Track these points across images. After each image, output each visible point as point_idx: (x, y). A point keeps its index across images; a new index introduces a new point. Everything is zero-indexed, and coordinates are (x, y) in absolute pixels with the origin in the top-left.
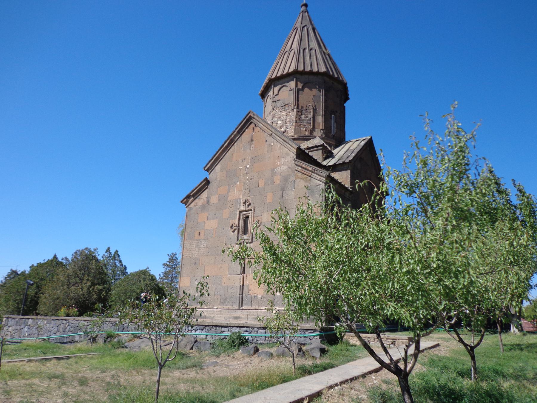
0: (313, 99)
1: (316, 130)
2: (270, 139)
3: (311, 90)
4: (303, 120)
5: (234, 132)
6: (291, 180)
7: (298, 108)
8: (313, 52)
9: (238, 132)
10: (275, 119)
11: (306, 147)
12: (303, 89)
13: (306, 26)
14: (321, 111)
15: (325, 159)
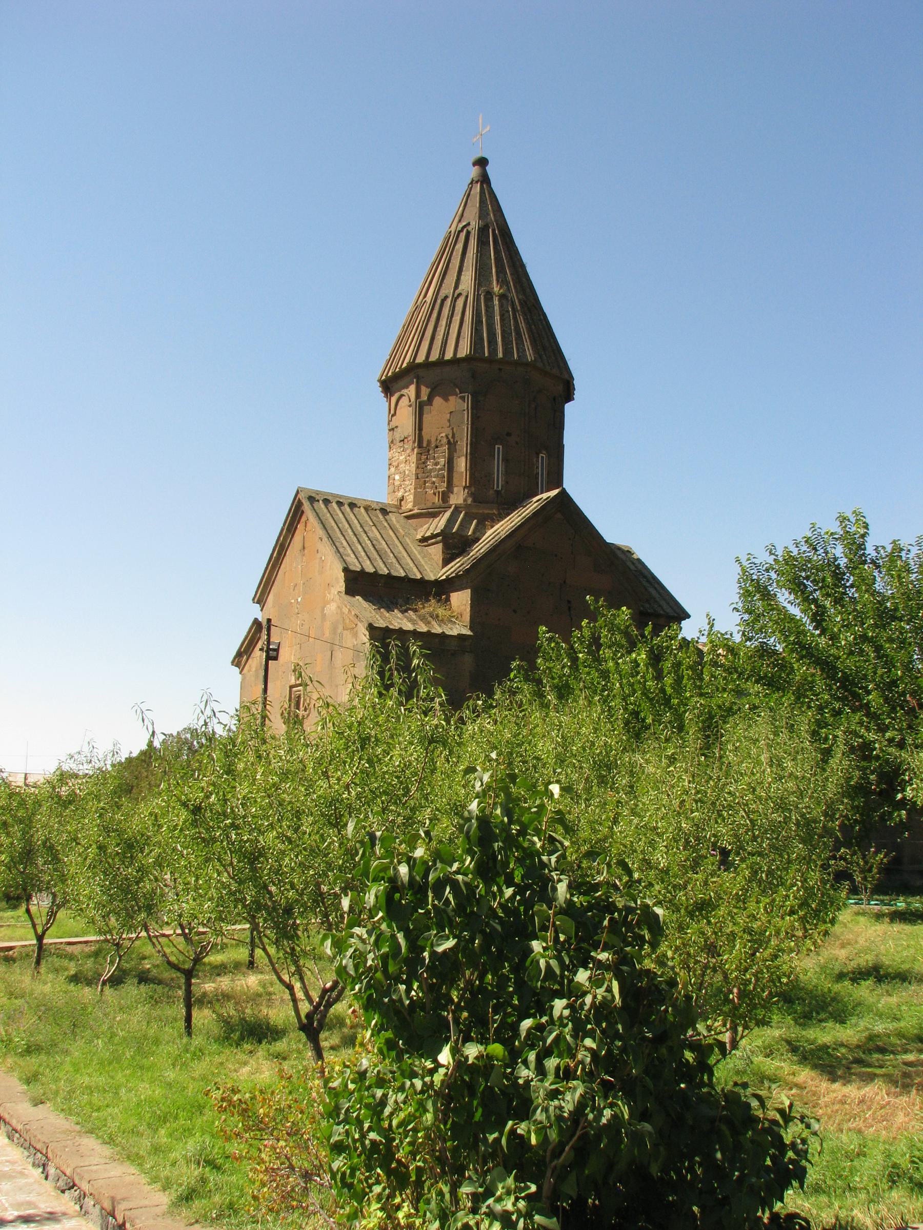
0: (449, 421)
1: (455, 489)
2: (320, 546)
3: (447, 400)
4: (431, 470)
5: (282, 530)
6: (339, 631)
7: (420, 446)
8: (460, 303)
9: (289, 530)
10: (393, 469)
11: (419, 537)
12: (430, 401)
13: (469, 224)
14: (464, 446)
15: (446, 562)
